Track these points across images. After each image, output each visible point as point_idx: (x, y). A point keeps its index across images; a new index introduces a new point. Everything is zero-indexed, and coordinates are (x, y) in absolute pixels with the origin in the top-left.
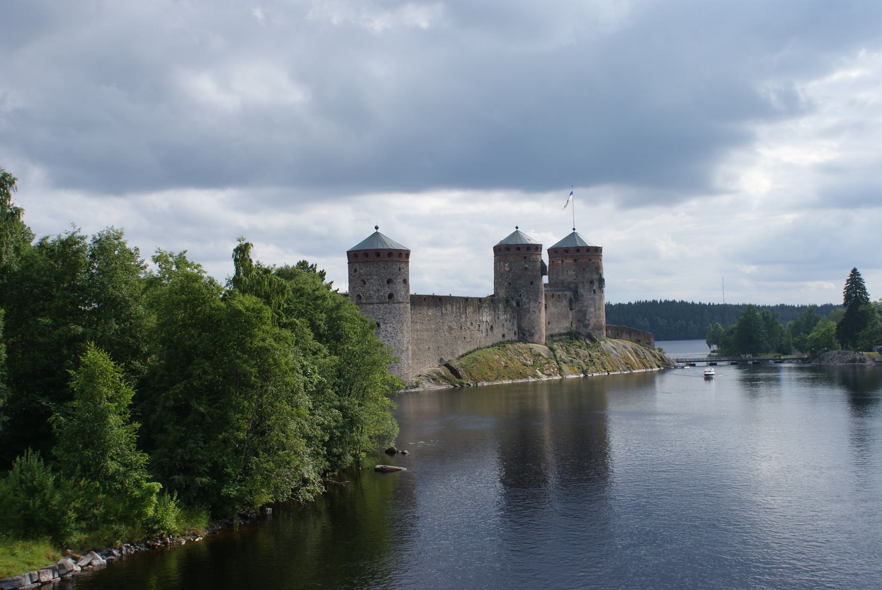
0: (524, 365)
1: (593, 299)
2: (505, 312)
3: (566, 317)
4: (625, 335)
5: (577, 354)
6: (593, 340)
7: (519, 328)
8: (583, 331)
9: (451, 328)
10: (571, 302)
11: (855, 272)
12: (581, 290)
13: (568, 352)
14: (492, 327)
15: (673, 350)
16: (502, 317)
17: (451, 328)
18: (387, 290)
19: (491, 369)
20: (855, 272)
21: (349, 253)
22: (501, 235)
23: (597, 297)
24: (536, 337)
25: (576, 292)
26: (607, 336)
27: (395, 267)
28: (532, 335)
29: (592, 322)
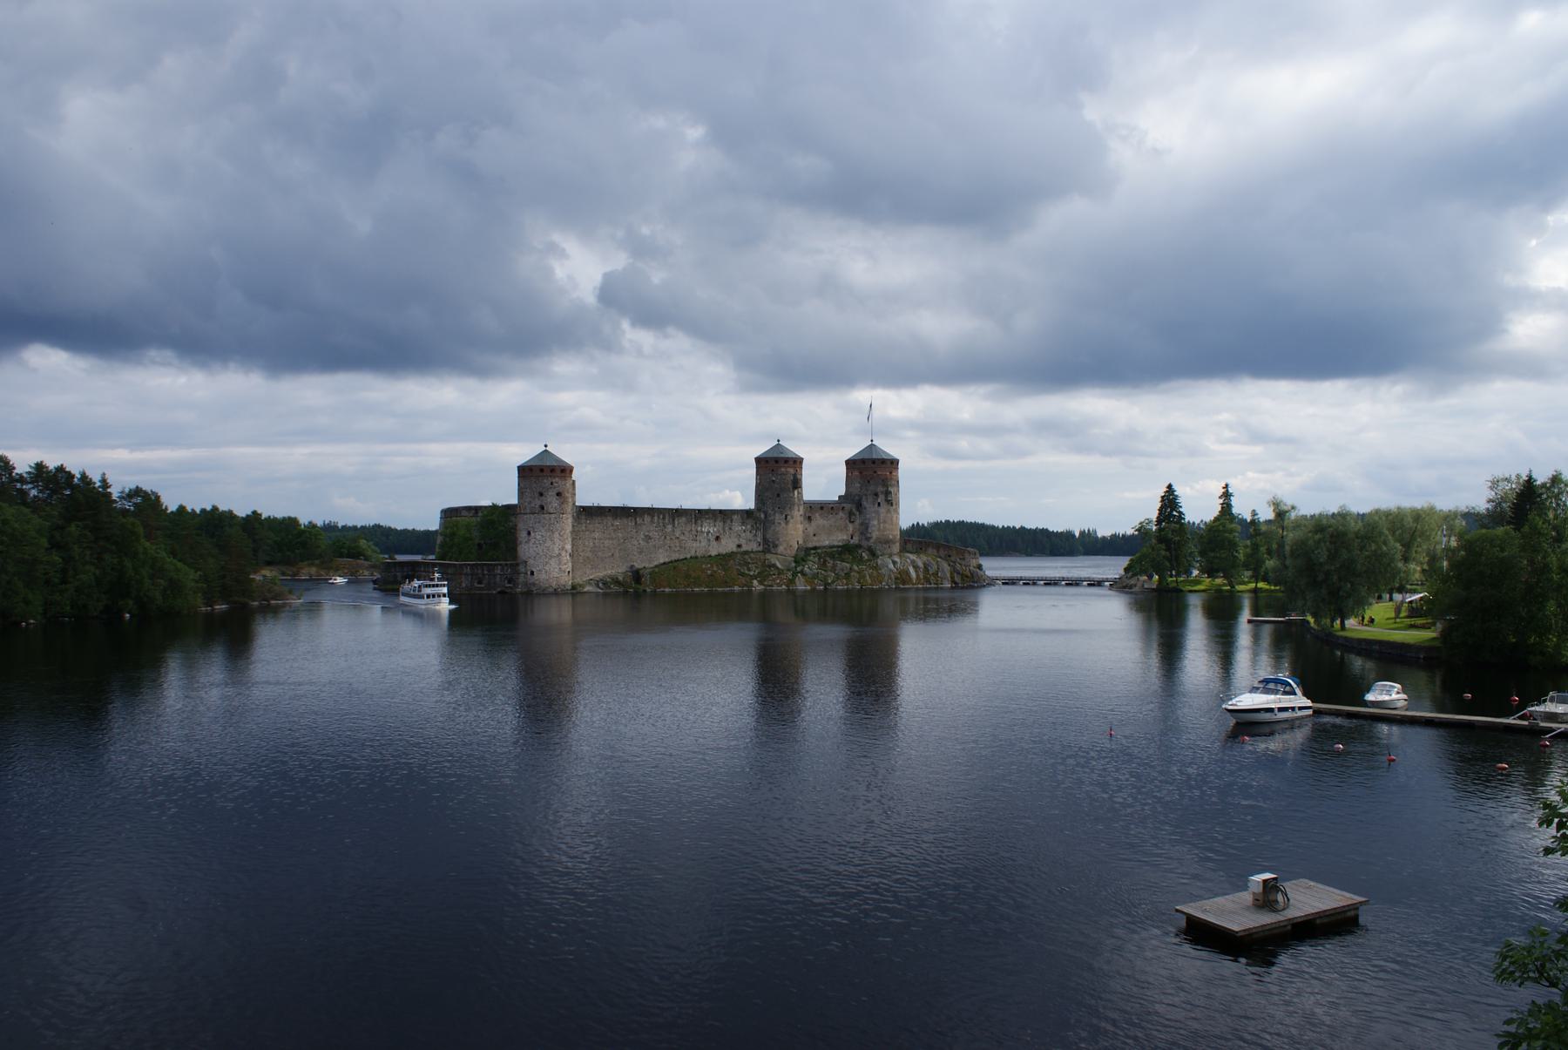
0: (743, 575)
1: (877, 513)
2: (743, 523)
3: (843, 529)
4: (930, 550)
5: (834, 569)
6: (873, 554)
7: (765, 539)
8: (864, 543)
9: (648, 538)
10: (851, 514)
11: (1170, 486)
12: (864, 503)
13: (823, 565)
14: (717, 538)
15: (993, 567)
16: (737, 527)
17: (648, 538)
18: (538, 502)
19: (687, 576)
20: (1170, 486)
21: (847, 462)
22: (761, 449)
23: (882, 510)
24: (781, 549)
25: (859, 506)
26: (903, 550)
27: (547, 482)
28: (776, 546)
29: (875, 535)
